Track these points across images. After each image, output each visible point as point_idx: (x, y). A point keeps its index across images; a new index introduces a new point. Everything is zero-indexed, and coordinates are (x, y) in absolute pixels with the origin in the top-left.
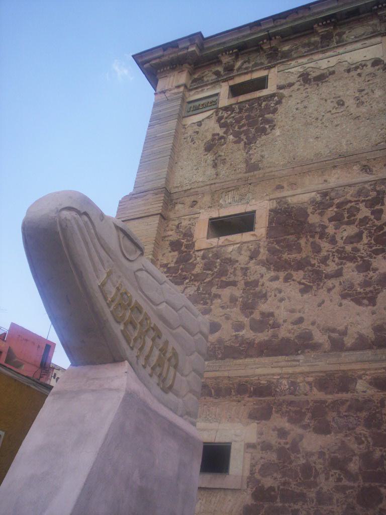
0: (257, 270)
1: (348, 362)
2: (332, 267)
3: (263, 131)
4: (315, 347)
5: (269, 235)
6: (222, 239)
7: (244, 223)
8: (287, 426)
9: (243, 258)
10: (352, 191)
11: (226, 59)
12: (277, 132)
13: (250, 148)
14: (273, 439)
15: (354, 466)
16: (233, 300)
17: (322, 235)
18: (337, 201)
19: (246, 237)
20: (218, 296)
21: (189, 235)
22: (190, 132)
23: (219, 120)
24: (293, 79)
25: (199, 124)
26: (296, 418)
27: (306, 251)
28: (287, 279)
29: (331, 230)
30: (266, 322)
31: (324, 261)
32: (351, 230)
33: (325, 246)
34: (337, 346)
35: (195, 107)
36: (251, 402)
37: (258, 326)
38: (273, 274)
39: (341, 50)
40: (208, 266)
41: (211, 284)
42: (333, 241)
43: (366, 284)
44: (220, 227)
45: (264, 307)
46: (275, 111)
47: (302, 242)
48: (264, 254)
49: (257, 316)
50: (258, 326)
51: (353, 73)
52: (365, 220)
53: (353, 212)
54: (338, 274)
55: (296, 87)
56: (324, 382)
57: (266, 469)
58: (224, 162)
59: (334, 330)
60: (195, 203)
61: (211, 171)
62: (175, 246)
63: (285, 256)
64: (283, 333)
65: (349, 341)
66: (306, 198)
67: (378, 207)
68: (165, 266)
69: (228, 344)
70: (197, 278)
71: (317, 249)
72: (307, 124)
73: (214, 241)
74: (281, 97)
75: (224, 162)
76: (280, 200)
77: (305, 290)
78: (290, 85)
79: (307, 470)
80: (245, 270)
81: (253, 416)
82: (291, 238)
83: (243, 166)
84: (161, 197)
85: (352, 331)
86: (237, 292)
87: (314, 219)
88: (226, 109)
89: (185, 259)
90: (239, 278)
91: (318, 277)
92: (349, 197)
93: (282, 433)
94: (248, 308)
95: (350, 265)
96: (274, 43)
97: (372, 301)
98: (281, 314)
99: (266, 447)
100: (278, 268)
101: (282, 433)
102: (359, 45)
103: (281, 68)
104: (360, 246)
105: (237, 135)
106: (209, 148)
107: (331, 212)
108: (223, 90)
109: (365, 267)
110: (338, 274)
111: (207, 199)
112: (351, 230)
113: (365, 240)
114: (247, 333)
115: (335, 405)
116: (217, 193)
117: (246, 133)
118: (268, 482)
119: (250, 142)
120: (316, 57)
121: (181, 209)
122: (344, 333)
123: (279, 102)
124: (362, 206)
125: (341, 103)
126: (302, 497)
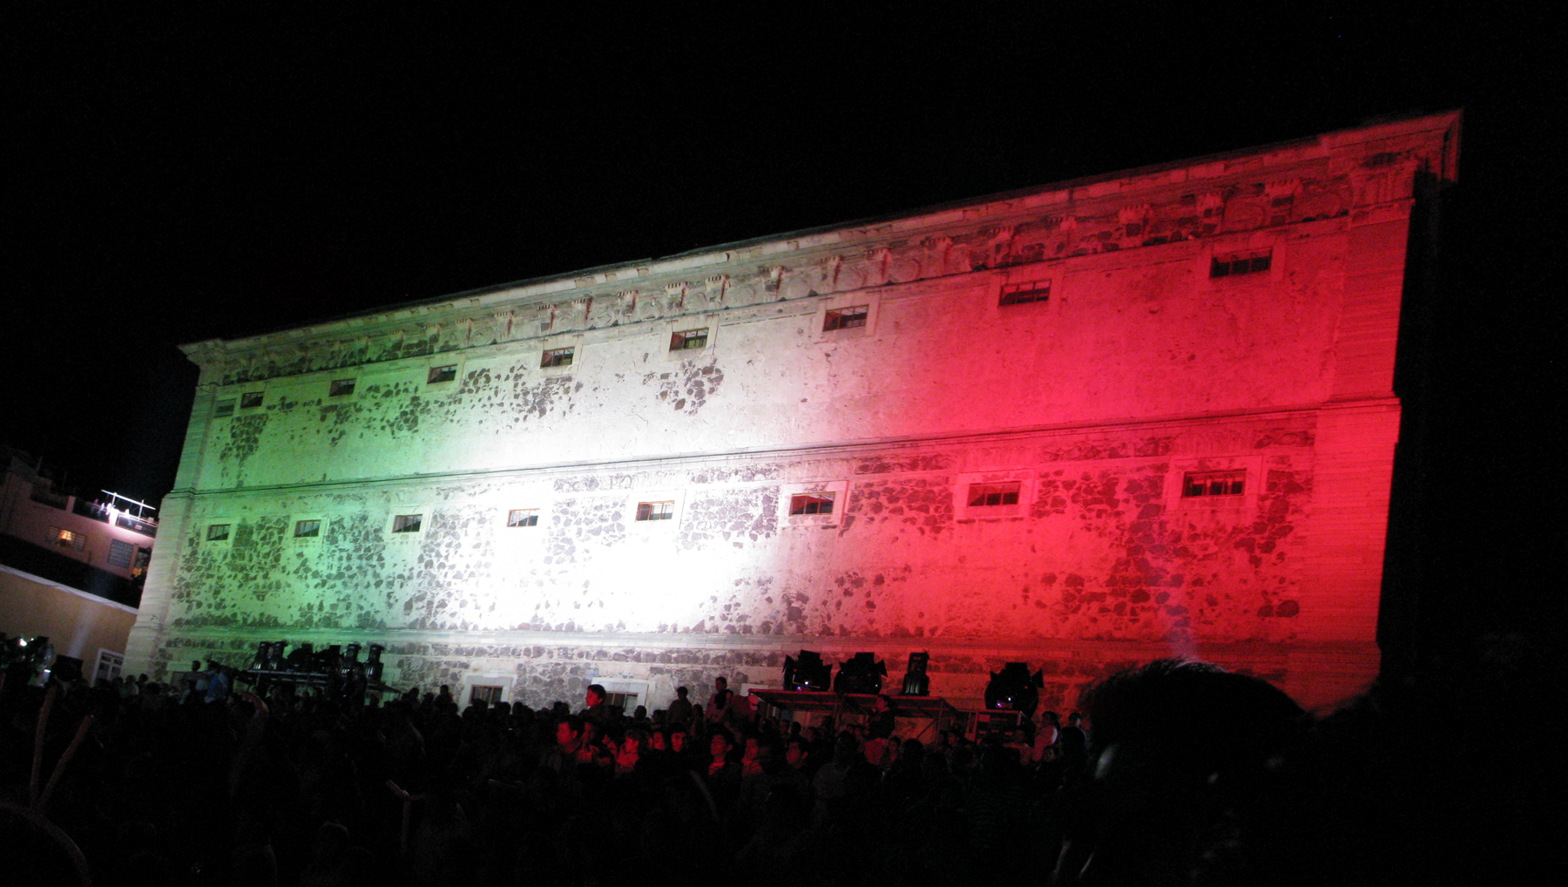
2: (252, 574)
5: (234, 546)
9: (220, 559)
13: (246, 463)
16: (211, 587)
17: (255, 551)
18: (267, 525)
20: (204, 584)
31: (252, 568)
32: (267, 549)
33: (255, 558)
38: (229, 573)
40: (204, 561)
47: (246, 552)
48: (229, 559)
49: (218, 600)
50: (220, 606)
59: (245, 613)
65: (249, 622)
67: (281, 535)
68: (184, 556)
69: (204, 616)
82: (242, 548)
85: (251, 615)
86: (213, 583)
89: (194, 553)
91: (247, 578)
92: (271, 524)
98: (228, 602)
100: (232, 570)
104: (268, 561)
110: (255, 578)
113: (271, 558)
114: (213, 611)
122: (249, 616)
124: (276, 532)
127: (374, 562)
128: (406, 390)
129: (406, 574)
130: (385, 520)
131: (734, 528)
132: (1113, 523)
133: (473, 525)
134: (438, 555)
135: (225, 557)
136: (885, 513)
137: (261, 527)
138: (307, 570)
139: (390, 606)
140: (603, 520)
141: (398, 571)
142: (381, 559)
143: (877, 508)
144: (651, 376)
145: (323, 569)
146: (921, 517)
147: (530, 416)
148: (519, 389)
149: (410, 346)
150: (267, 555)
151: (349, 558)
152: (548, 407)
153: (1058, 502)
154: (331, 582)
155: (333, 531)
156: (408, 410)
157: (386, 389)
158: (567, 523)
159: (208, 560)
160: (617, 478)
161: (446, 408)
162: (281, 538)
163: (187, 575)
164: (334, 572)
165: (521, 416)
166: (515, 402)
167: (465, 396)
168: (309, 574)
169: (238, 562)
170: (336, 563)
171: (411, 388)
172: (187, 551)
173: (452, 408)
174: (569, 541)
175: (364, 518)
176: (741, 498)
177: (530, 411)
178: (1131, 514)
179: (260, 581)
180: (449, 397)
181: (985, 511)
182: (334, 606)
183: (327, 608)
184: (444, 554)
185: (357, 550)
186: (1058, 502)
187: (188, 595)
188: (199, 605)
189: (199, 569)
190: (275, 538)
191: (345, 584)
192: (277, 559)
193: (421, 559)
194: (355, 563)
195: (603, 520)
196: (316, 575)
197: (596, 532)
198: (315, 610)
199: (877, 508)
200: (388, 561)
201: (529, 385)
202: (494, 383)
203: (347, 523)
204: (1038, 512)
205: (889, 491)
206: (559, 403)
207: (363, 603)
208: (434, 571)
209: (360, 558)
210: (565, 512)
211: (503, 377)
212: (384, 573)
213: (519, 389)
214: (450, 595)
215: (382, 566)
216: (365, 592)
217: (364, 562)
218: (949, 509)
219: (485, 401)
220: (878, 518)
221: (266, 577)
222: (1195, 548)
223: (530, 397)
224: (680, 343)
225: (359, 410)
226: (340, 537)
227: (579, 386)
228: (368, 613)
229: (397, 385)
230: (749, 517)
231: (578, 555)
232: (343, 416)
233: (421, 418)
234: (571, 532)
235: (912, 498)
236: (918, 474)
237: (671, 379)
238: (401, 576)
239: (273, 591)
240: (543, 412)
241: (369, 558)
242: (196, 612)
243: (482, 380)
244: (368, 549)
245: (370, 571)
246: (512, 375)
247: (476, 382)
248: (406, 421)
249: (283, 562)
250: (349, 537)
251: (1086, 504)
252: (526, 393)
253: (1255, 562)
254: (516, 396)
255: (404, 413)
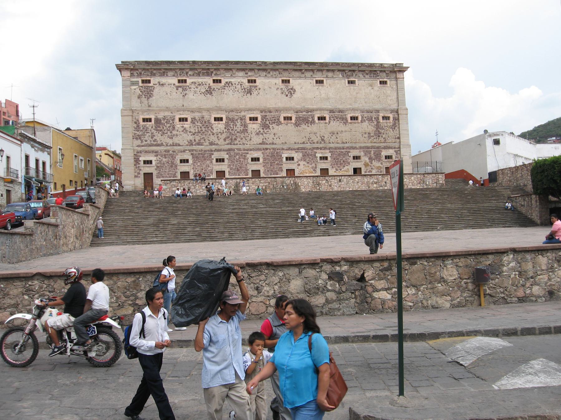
0: (153, 131)
1: (168, 148)
2: (166, 132)
3: (151, 96)
4: (164, 145)
6: (146, 123)
7: (150, 120)
8: (160, 157)
9: (150, 128)
10: (169, 117)
11: (140, 71)
12: (154, 98)
14: (159, 159)
15: (170, 163)
16: (149, 136)
19: (150, 123)
21: (138, 121)
22: (133, 92)
23: (140, 89)
24: (157, 83)
25: (135, 89)
26: (162, 156)
27: (162, 128)
28: (159, 133)
29: (165, 124)
30: (155, 141)
31: (165, 130)
32: (169, 125)
33: (165, 127)
34: (167, 145)
35: (133, 84)
36: (155, 154)
37: (154, 141)
39: (167, 78)
40: (144, 128)
41: (144, 132)
42: (166, 127)
43: (171, 135)
44: (145, 120)
45: (155, 138)
46: (153, 91)
48: (154, 127)
50: (154, 141)
51: (170, 86)
52: (171, 124)
53: (169, 121)
54: (167, 133)
55: (157, 85)
56: (165, 151)
57: (158, 163)
58: (143, 103)
60: (138, 113)
61: (140, 105)
62: (136, 123)
63: (158, 128)
64: (158, 143)
65: (169, 145)
66: (161, 117)
70: (141, 131)
71: (163, 128)
72: (160, 98)
73: (144, 123)
74: (154, 87)
75: (143, 103)
76: (156, 116)
77: (162, 135)
78: (156, 84)
79: (164, 163)
80: (151, 130)
81: (155, 156)
83: (147, 105)
84: (131, 111)
86: (150, 135)
87: (162, 121)
88: (141, 87)
89: (138, 126)
90: (150, 132)
91: (164, 133)
93: (160, 158)
94: (152, 138)
95: (169, 132)
96: (152, 70)
97: (172, 139)
98: (158, 139)
99: (158, 160)
101: (160, 158)
102: (171, 78)
103: (154, 78)
105: (145, 95)
106: (139, 98)
107: (166, 120)
108: (140, 80)
109: (171, 132)
110: (167, 133)
111: (140, 113)
112: (169, 125)
115: (167, 154)
116: (143, 112)
117: (147, 95)
118: (158, 165)
119: (148, 98)
120: (162, 78)
121: (135, 114)
123: (154, 89)
125: (167, 94)
126: (163, 167)
127: (210, 128)
128: (206, 84)
129: (222, 132)
130: (210, 118)
131: (306, 123)
132: (373, 124)
133: (239, 120)
134: (231, 127)
135: (152, 127)
136: (336, 121)
137: (164, 119)
138: (187, 131)
139: (219, 140)
140: (275, 120)
141: (219, 131)
142: (212, 128)
143: (334, 120)
144: (278, 88)
145: (193, 130)
146: (342, 122)
147: (248, 95)
148: (242, 88)
149: (203, 73)
150: (170, 127)
151: (201, 128)
152: (252, 93)
153: (364, 120)
154: (197, 134)
155: (193, 121)
156: (208, 89)
157: (198, 83)
158: (266, 121)
159: (146, 129)
160: (276, 111)
161: (221, 90)
162: (173, 122)
163: (138, 133)
164: (197, 131)
165: (245, 94)
166: (242, 91)
167: (226, 87)
168: (188, 132)
169: (158, 128)
170: (197, 129)
171: (208, 84)
172: (135, 125)
173: (223, 90)
174: (267, 124)
175: (203, 118)
176: (306, 117)
177: (248, 93)
178: (375, 123)
179: (170, 134)
180: (221, 87)
181: (353, 121)
182: (199, 140)
183: (197, 141)
184: (232, 127)
185: (203, 126)
186: (364, 120)
187: (140, 138)
188: (146, 141)
189: (141, 131)
190: (171, 122)
191: (201, 134)
192: (174, 128)
193: (225, 128)
194: (204, 129)
195: (275, 120)
196: (190, 132)
197: (274, 123)
198: (193, 141)
199: (334, 120)
200: (215, 129)
201: (245, 87)
202: (234, 85)
203: (197, 118)
204: (362, 122)
205: (336, 117)
206: (255, 92)
207: (209, 139)
208: (231, 131)
209: (205, 128)
210: (265, 118)
211: (237, 84)
212: (214, 131)
213: (242, 88)
214: (237, 137)
215: (213, 130)
216: (209, 136)
217: (206, 129)
218: (347, 120)
219: (233, 89)
220: (335, 122)
221: (171, 132)
222: (385, 128)
223: (246, 90)
224: (283, 81)
225: (190, 88)
226: (196, 122)
227: (259, 89)
228: (212, 142)
229: (202, 83)
230: (309, 121)
231: (271, 127)
232: (185, 90)
233: (213, 92)
234: (268, 123)
235: (340, 118)
236: (340, 114)
237: (283, 90)
238: (220, 132)
239: (175, 136)
240: (251, 94)
241: (208, 128)
242: (144, 143)
243: (230, 85)
244: (207, 126)
245: (209, 132)
246: (239, 84)
247: (228, 85)
248: (208, 93)
249: (176, 128)
250: (199, 122)
251: (369, 121)
252: (245, 89)
253: (393, 131)
254: (242, 89)
255: (206, 90)
